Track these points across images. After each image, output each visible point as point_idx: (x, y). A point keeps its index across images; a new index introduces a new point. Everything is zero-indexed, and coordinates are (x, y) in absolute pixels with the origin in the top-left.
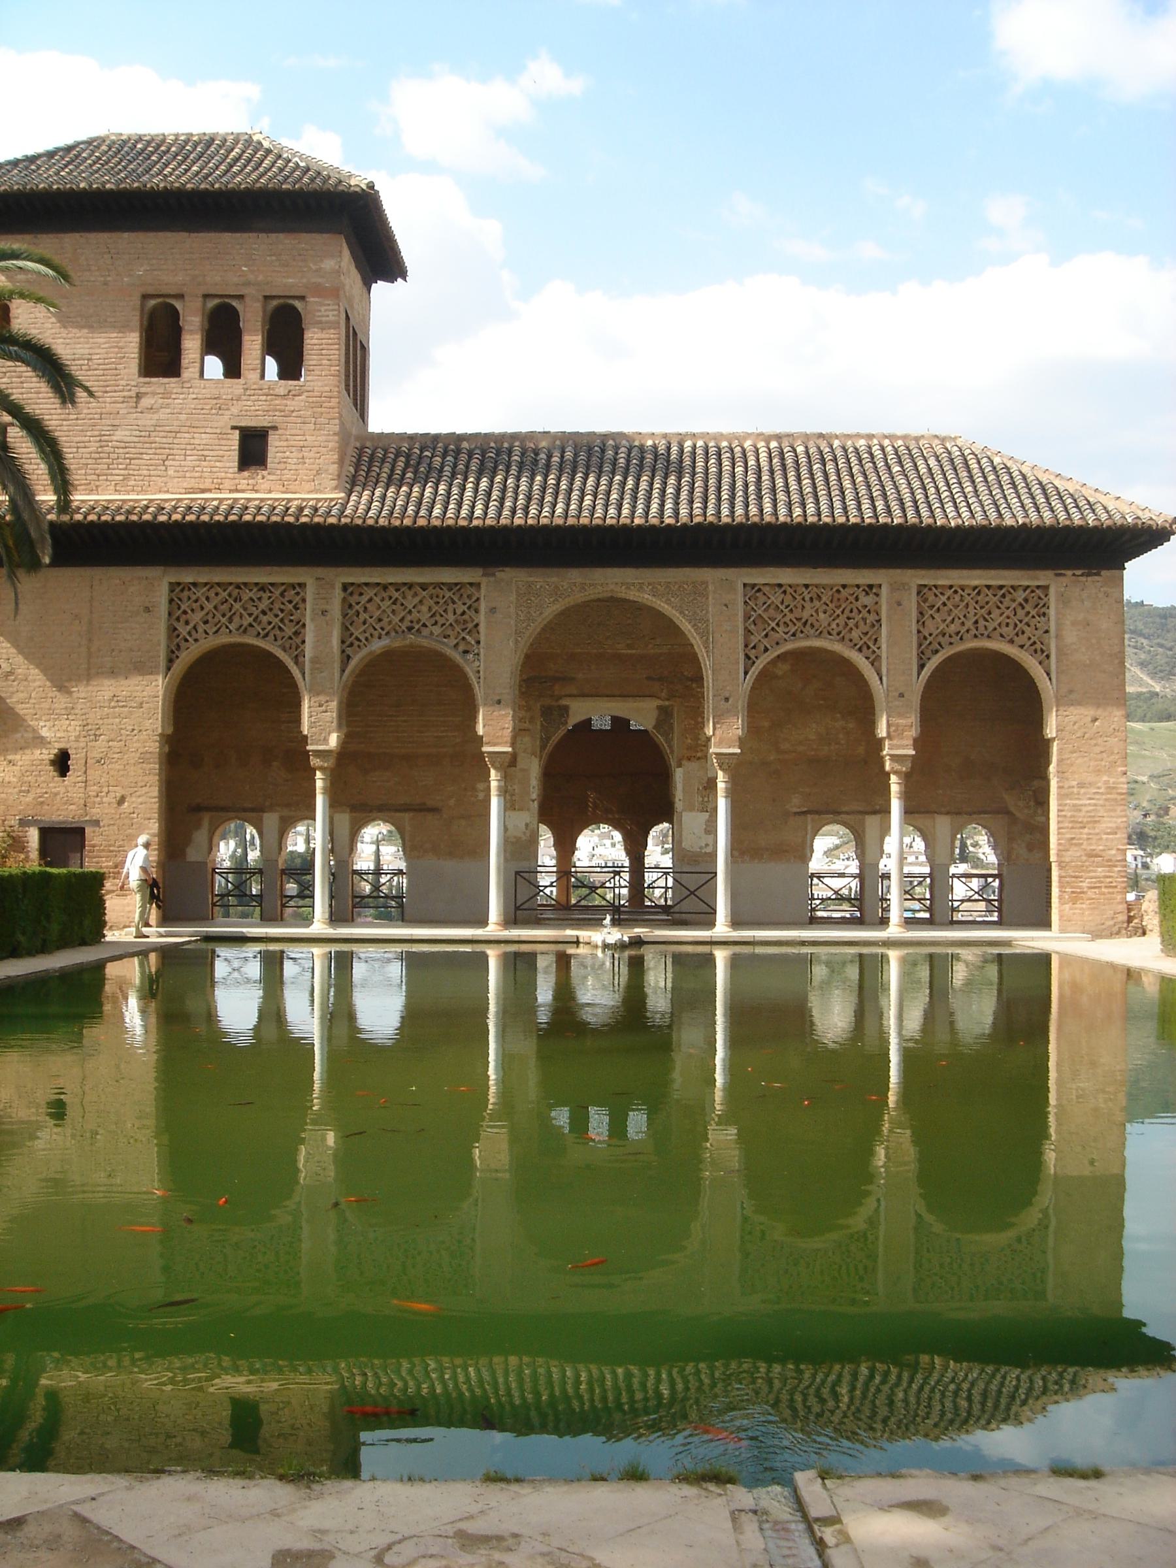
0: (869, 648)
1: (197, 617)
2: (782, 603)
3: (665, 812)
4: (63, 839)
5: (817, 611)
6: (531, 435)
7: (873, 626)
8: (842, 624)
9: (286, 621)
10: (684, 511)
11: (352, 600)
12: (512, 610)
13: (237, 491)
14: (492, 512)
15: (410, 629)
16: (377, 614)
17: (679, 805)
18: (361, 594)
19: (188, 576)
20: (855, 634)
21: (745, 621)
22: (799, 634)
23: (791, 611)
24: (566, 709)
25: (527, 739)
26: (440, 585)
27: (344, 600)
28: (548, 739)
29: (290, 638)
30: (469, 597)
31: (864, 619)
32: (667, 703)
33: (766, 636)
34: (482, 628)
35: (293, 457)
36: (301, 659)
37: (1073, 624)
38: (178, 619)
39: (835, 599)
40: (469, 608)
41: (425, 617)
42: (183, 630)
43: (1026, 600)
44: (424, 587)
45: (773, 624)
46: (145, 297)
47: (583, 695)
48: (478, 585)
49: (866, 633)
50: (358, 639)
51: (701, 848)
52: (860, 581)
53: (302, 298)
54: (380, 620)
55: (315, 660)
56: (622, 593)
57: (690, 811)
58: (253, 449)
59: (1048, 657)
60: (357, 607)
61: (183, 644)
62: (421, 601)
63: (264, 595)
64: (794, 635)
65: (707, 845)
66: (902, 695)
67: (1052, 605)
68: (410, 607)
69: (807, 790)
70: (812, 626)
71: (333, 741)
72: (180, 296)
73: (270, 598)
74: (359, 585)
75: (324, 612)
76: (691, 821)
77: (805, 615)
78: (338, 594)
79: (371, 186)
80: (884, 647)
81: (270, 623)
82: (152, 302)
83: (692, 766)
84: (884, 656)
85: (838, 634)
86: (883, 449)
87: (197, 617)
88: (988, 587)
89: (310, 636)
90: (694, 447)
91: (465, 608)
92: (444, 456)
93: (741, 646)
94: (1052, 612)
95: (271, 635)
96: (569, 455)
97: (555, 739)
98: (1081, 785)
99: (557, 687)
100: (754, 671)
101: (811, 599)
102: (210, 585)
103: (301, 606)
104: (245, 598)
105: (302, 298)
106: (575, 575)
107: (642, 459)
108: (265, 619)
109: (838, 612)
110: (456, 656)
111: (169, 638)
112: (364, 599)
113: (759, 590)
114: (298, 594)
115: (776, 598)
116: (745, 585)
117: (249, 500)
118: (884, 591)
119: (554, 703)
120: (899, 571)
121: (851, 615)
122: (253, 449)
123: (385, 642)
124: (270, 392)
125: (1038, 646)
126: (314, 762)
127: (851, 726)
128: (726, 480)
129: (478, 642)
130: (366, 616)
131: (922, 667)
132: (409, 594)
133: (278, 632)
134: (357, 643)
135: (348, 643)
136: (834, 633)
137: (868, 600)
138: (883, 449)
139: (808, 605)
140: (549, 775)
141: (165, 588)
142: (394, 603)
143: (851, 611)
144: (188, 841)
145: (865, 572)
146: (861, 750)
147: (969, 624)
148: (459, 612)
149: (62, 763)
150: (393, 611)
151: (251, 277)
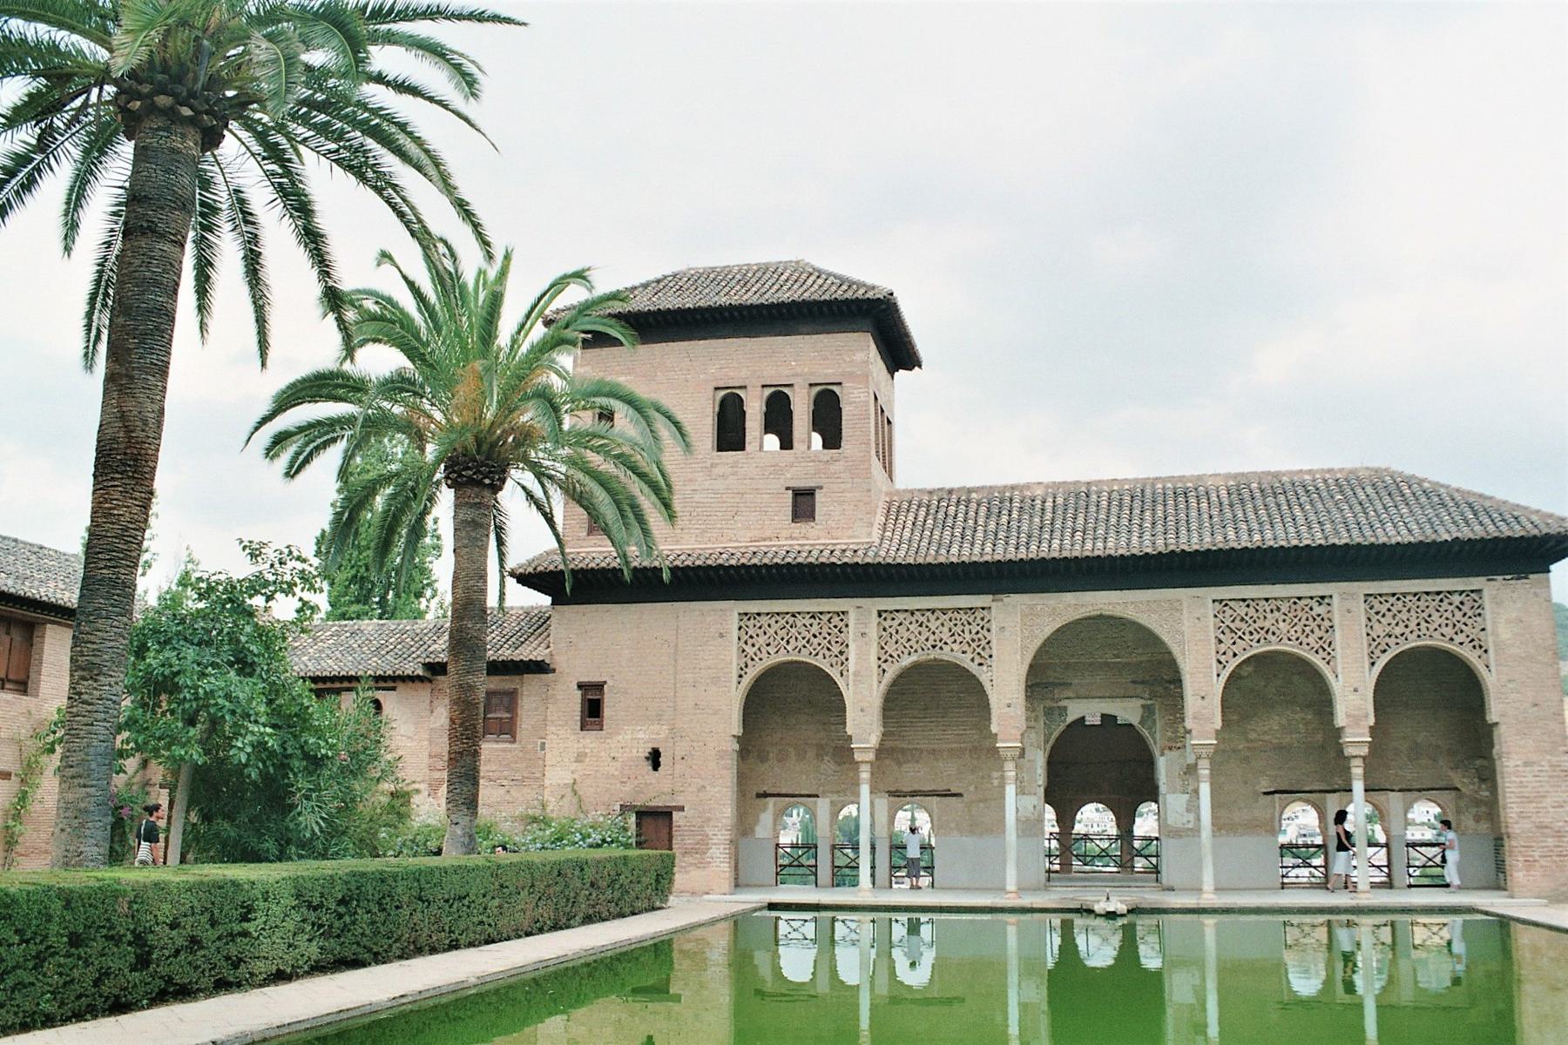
1: (762, 640)
3: (1153, 795)
4: (655, 821)
6: (1028, 486)
10: (1160, 542)
13: (791, 538)
16: (906, 635)
17: (1163, 789)
19: (753, 606)
20: (1311, 640)
25: (1033, 735)
37: (1509, 621)
41: (946, 636)
55: (855, 674)
58: (803, 503)
66: (1356, 690)
67: (1487, 605)
69: (1273, 773)
76: (1174, 801)
77: (1267, 624)
80: (1338, 649)
82: (722, 393)
83: (1175, 753)
86: (1325, 481)
87: (762, 640)
88: (1427, 593)
89: (852, 653)
94: (1487, 613)
96: (1060, 501)
97: (1056, 735)
98: (1526, 764)
100: (1226, 674)
104: (799, 624)
106: (1069, 598)
108: (815, 641)
110: (973, 668)
111: (739, 658)
115: (1241, 610)
118: (1335, 600)
122: (803, 503)
123: (914, 658)
124: (815, 459)
126: (858, 757)
128: (1194, 514)
132: (932, 618)
138: (1325, 481)
139: (1269, 615)
144: (757, 821)
146: (1319, 737)
147: (1412, 626)
149: (655, 758)
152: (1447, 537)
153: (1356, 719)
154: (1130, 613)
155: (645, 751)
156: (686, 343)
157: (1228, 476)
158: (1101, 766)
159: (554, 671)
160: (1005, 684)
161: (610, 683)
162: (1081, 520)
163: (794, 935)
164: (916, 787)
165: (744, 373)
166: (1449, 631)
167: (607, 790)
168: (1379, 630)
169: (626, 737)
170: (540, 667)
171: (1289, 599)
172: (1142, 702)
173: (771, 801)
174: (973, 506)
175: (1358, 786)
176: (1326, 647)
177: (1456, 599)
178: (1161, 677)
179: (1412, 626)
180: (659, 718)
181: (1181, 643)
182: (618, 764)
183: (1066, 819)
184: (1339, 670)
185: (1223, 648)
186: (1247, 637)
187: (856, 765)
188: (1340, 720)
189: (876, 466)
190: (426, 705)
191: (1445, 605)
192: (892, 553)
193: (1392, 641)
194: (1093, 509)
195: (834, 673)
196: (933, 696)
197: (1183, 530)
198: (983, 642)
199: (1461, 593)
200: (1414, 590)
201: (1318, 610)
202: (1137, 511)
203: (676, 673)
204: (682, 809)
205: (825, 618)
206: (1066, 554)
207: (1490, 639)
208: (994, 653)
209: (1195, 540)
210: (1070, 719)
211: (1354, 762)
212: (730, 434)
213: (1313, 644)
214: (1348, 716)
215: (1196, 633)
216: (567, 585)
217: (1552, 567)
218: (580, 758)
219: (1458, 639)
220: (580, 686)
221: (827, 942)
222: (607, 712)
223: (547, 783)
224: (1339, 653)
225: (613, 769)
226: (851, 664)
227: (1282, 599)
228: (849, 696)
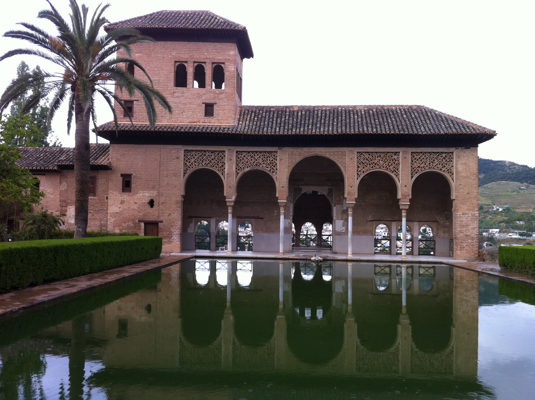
1: (193, 160)
6: (292, 107)
10: (339, 130)
11: (239, 156)
12: (287, 159)
13: (204, 123)
15: (256, 165)
17: (334, 218)
19: (190, 148)
20: (391, 167)
22: (374, 168)
24: (301, 189)
26: (265, 152)
30: (274, 156)
34: (278, 165)
35: (221, 112)
37: (461, 164)
38: (187, 161)
42: (188, 164)
43: (446, 156)
44: (260, 152)
46: (176, 62)
48: (277, 152)
52: (393, 151)
53: (224, 63)
55: (228, 174)
56: (319, 154)
58: (209, 109)
59: (453, 174)
61: (188, 168)
66: (406, 186)
71: (234, 198)
72: (186, 62)
75: (231, 160)
76: (339, 223)
77: (376, 161)
79: (245, 28)
80: (400, 171)
82: (178, 64)
83: (339, 206)
84: (400, 174)
86: (400, 110)
87: (193, 160)
88: (434, 153)
89: (226, 166)
90: (341, 110)
92: (266, 113)
93: (356, 171)
94: (454, 160)
98: (463, 214)
100: (360, 179)
102: (197, 151)
104: (207, 155)
105: (224, 63)
106: (306, 149)
107: (326, 114)
108: (213, 161)
111: (184, 166)
112: (243, 156)
115: (367, 156)
117: (209, 125)
118: (401, 154)
122: (209, 109)
123: (249, 169)
124: (214, 92)
125: (449, 171)
126: (228, 204)
131: (412, 177)
135: (238, 169)
137: (396, 157)
138: (400, 110)
139: (376, 158)
141: (183, 151)
144: (188, 227)
145: (395, 148)
147: (427, 164)
149: (151, 203)
151: (208, 56)
152: (442, 132)
153: (404, 196)
154: (327, 155)
155: (147, 200)
156: (163, 42)
157: (365, 106)
159: (111, 169)
160: (281, 179)
161: (134, 174)
162: (311, 121)
163: (202, 267)
165: (186, 56)
166: (440, 166)
167: (133, 215)
168: (415, 165)
169: (142, 196)
170: (106, 168)
171: (384, 153)
173: (194, 220)
174: (272, 113)
175: (404, 220)
176: (396, 170)
177: (444, 155)
178: (336, 179)
179: (427, 164)
180: (153, 188)
181: (345, 167)
182: (137, 205)
183: (298, 228)
184: (400, 179)
185: (360, 169)
186: (368, 166)
187: (227, 207)
188: (399, 196)
189: (237, 96)
190: (58, 181)
191: (440, 157)
193: (420, 169)
194: (315, 117)
195: (219, 173)
196: (256, 184)
198: (274, 164)
199: (446, 153)
200: (430, 151)
201: (394, 157)
202: (331, 118)
203: (160, 171)
204: (162, 222)
205: (217, 153)
207: (454, 170)
208: (278, 168)
210: (302, 192)
211: (403, 211)
212: (181, 80)
214: (402, 195)
215: (351, 165)
216: (114, 134)
217: (480, 145)
218: (122, 202)
219: (443, 169)
220: (122, 175)
221: (213, 269)
222: (133, 186)
223: (109, 212)
224: (400, 173)
225: (135, 207)
226: (226, 171)
227: (382, 153)
228: (225, 182)
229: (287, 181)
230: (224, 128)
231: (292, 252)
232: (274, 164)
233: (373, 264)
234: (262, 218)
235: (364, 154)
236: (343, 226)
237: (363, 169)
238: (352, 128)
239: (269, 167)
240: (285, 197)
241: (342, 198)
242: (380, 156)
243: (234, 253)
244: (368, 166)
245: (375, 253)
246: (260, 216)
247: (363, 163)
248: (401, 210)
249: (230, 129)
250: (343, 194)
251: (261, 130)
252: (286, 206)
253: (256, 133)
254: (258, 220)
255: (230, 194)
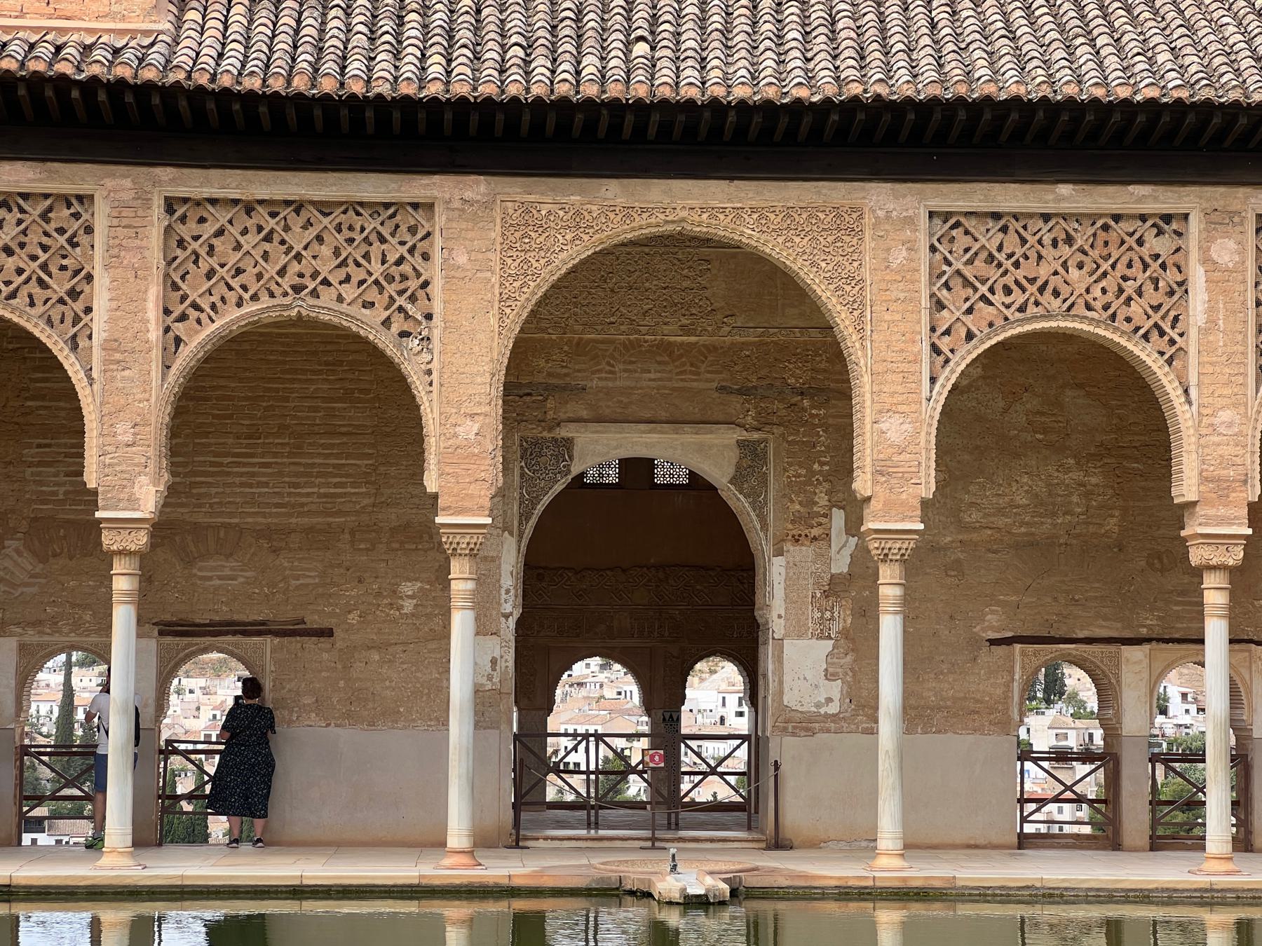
0: (1162, 334)
2: (1000, 249)
5: (1065, 265)
7: (1171, 293)
8: (1113, 289)
9: (54, 269)
11: (185, 231)
12: (495, 257)
14: (461, 68)
15: (297, 289)
16: (233, 258)
18: (202, 220)
20: (1135, 309)
21: (932, 284)
22: (1032, 310)
23: (1017, 265)
24: (568, 443)
26: (356, 206)
27: (168, 230)
28: (534, 502)
29: (61, 301)
30: (413, 230)
31: (1155, 281)
32: (756, 436)
33: (969, 311)
34: (436, 289)
36: (83, 343)
39: (1100, 242)
40: (411, 251)
41: (326, 267)
44: (324, 208)
45: (984, 289)
47: (599, 420)
49: (1156, 308)
50: (195, 306)
51: (818, 705)
54: (239, 271)
55: (111, 345)
56: (700, 224)
57: (800, 637)
60: (195, 245)
62: (319, 239)
63: (8, 216)
64: (1022, 309)
65: (829, 700)
68: (298, 247)
70: (1056, 293)
73: (20, 222)
74: (198, 203)
77: (1044, 272)
78: (157, 217)
80: (1193, 333)
81: (20, 271)
83: (805, 552)
84: (1192, 350)
85: (1106, 307)
89: (101, 296)
91: (404, 250)
95: (23, 293)
99: (550, 404)
100: (949, 377)
101: (1055, 243)
103: (83, 239)
106: (613, 191)
109: (1105, 266)
110: (385, 341)
112: (208, 229)
113: (957, 225)
114: (76, 216)
116: (931, 215)
119: (545, 434)
120: (1222, 190)
121: (1129, 273)
126: (109, 540)
127: (1094, 480)
129: (429, 317)
130: (213, 262)
132: (296, 222)
133: (36, 291)
134: (193, 314)
135: (176, 312)
136: (1098, 305)
139: (1048, 252)
140: (535, 572)
142: (268, 238)
143: (1130, 266)
146: (1112, 524)
148: (392, 258)
150: (265, 256)
153: (1218, 486)
154: (749, 234)
158: (644, 574)
164: (224, 612)
171: (1093, 218)
172: (745, 435)
176: (1166, 330)
178: (802, 383)
181: (857, 305)
184: (1193, 379)
186: (999, 298)
192: (207, 61)
196: (294, 408)
197: (874, 55)
198: (413, 284)
201: (1154, 244)
205: (35, 210)
206: (614, 91)
208: (437, 308)
209: (903, 75)
211: (1210, 580)
213: (1139, 318)
214: (1204, 479)
215: (894, 289)
226: (99, 323)
227: (1078, 218)
229: (497, 391)
230: (87, 49)
231: (517, 841)
232: (413, 284)
233: (1018, 911)
234: (327, 633)
235: (970, 224)
236: (829, 676)
237: (968, 320)
238: (900, 61)
239: (380, 300)
240: (483, 494)
241: (822, 500)
242: (1069, 240)
243: (149, 855)
244: (999, 298)
245: (1024, 841)
246: (314, 621)
247: (967, 283)
248: (1198, 573)
249: (128, 55)
250: (844, 469)
251: (329, 66)
252: (482, 559)
253: (300, 84)
254: (294, 643)
255: (126, 474)
